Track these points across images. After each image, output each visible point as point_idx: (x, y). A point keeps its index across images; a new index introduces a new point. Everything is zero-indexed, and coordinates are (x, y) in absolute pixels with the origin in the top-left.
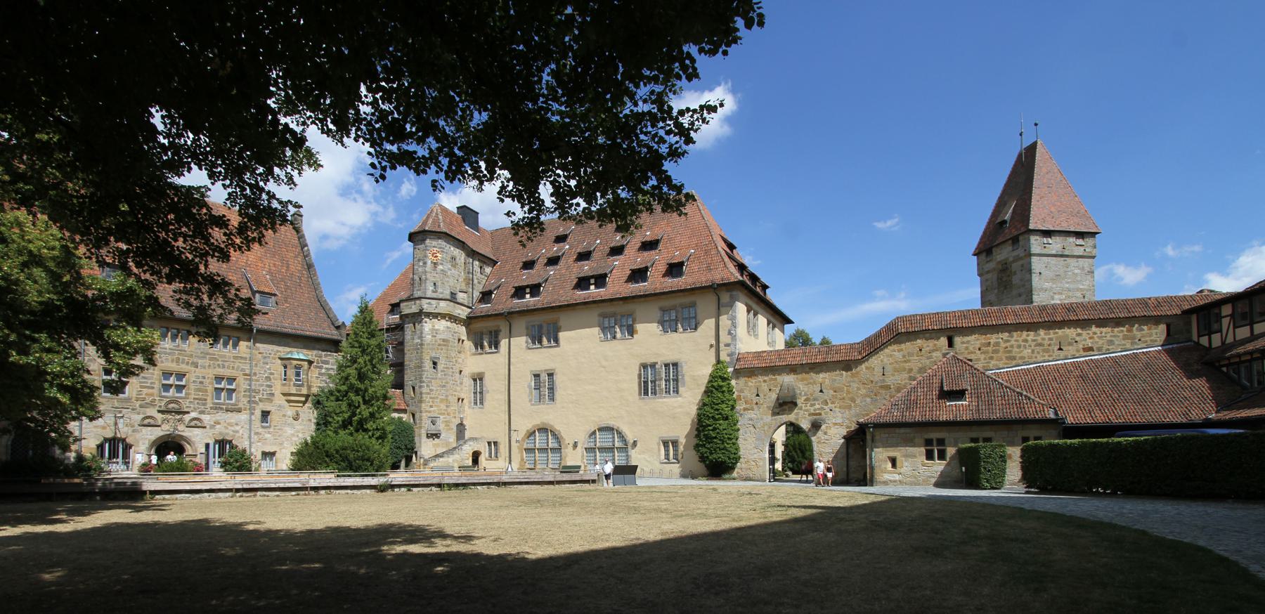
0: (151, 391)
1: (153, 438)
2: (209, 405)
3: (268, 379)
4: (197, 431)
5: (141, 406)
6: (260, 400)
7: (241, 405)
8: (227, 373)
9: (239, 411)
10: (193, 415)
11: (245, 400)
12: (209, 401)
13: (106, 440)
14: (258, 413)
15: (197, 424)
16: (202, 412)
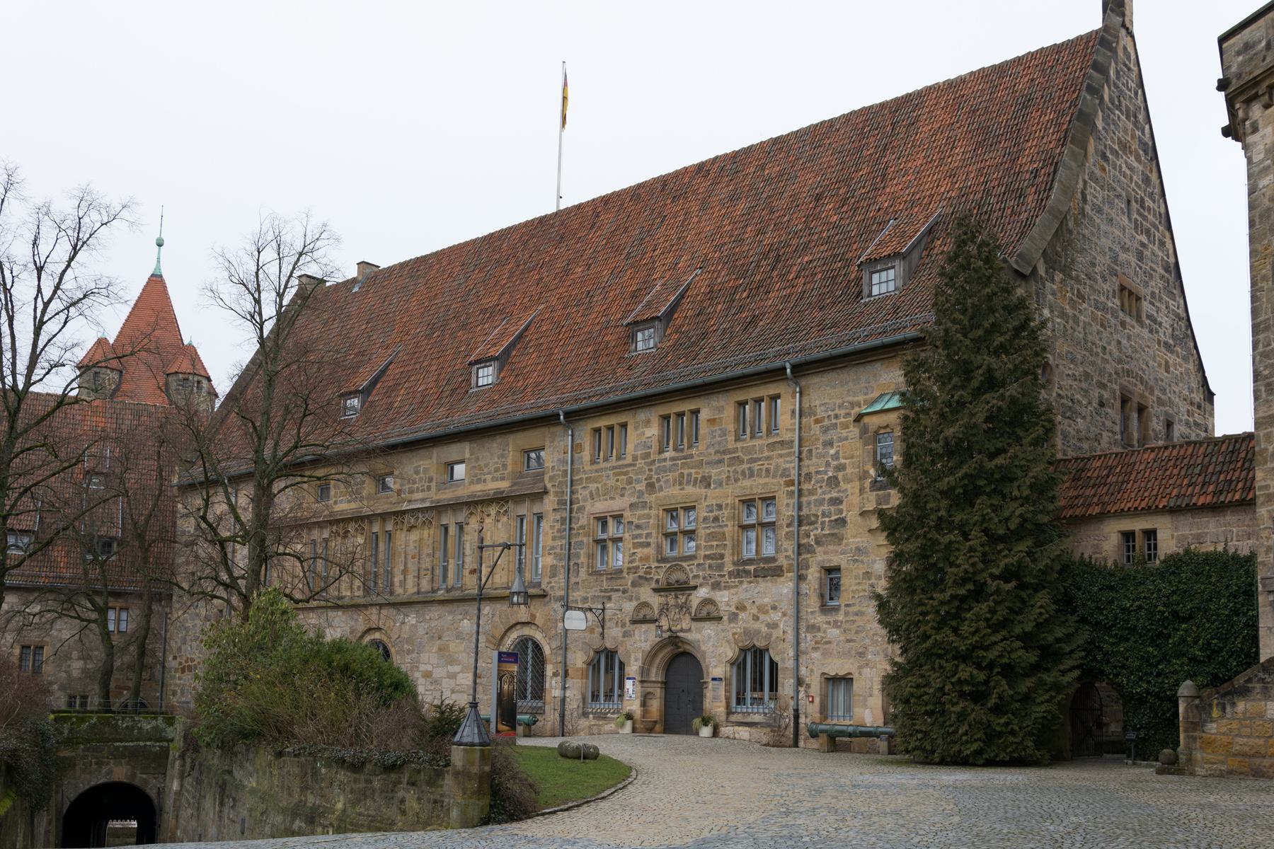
0: (646, 551)
1: (647, 646)
2: (729, 567)
3: (833, 482)
4: (709, 629)
5: (634, 584)
6: (818, 542)
7: (782, 561)
8: (755, 486)
9: (777, 572)
10: (703, 592)
11: (789, 547)
12: (728, 559)
13: (598, 652)
14: (813, 574)
15: (708, 614)
16: (716, 586)
